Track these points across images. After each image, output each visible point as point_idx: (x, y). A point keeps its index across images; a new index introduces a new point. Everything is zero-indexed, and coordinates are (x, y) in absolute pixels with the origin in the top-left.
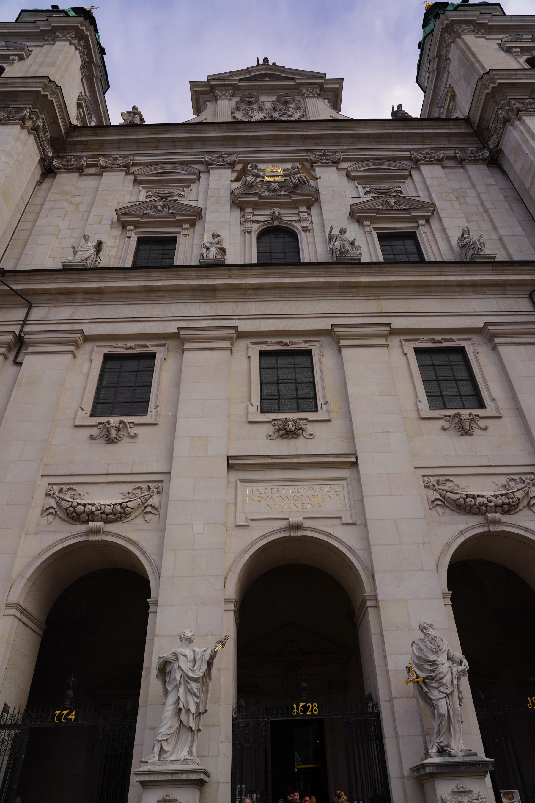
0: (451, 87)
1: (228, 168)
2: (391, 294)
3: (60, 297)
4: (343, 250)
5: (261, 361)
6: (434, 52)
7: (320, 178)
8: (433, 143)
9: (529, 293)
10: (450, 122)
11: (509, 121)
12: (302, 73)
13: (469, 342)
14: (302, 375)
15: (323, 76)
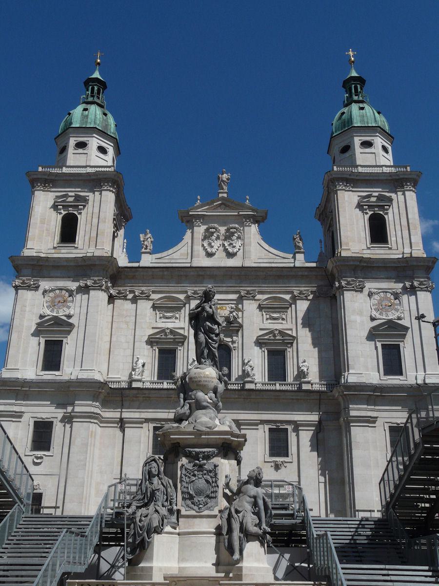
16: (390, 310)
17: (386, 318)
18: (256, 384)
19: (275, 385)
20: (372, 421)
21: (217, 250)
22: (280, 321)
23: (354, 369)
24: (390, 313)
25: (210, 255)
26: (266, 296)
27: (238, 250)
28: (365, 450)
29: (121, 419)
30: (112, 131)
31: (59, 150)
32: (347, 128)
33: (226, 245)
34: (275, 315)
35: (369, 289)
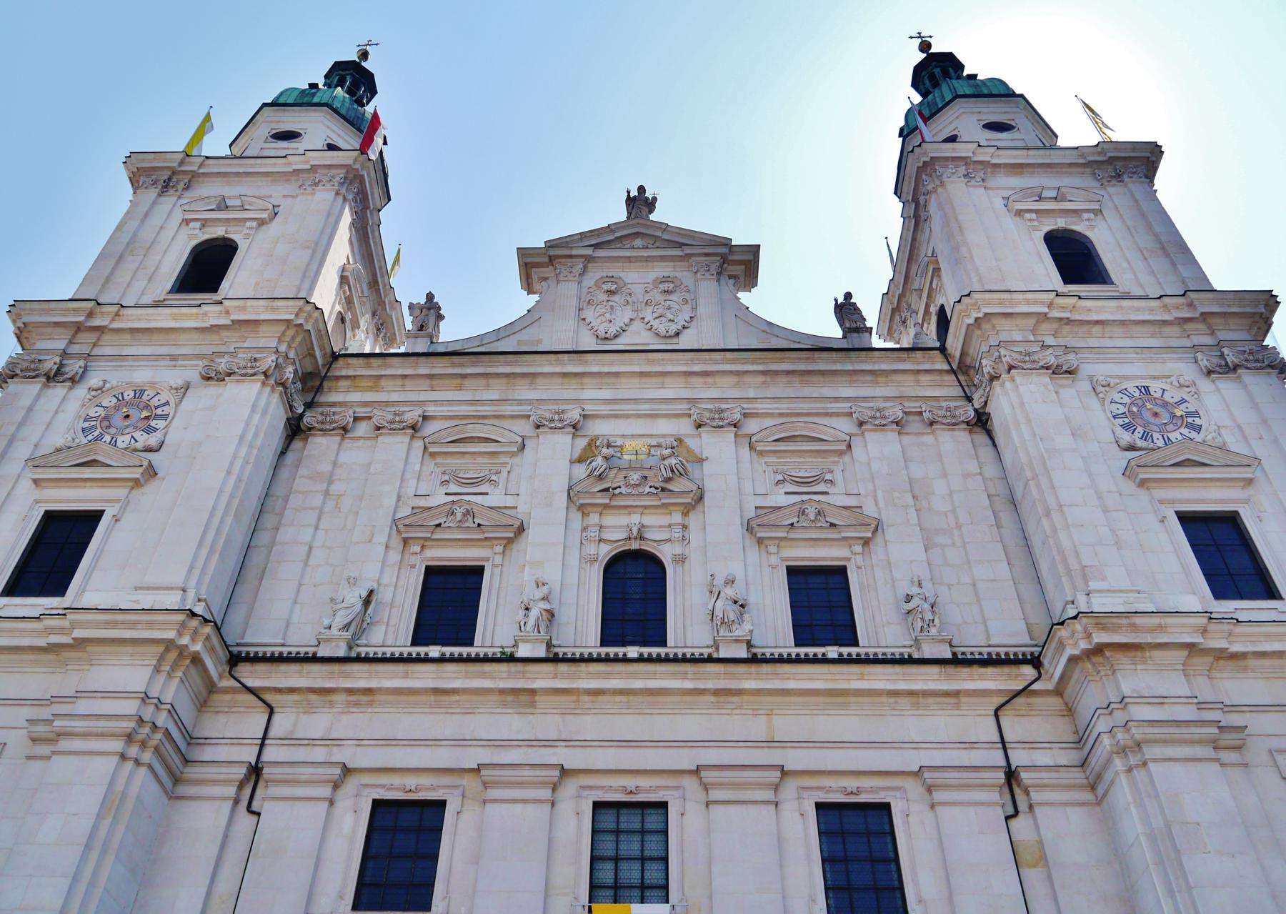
0: (935, 255)
1: (568, 433)
2: (790, 706)
3: (313, 697)
4: (726, 620)
5: (595, 818)
6: (908, 193)
7: (707, 458)
8: (890, 385)
9: (994, 708)
10: (918, 352)
11: (998, 378)
12: (694, 234)
13: (898, 794)
14: (653, 847)
15: (726, 242)
16: (1170, 427)
21: (621, 328)
23: (1104, 579)
27: (680, 328)
29: (255, 771)
33: (649, 315)
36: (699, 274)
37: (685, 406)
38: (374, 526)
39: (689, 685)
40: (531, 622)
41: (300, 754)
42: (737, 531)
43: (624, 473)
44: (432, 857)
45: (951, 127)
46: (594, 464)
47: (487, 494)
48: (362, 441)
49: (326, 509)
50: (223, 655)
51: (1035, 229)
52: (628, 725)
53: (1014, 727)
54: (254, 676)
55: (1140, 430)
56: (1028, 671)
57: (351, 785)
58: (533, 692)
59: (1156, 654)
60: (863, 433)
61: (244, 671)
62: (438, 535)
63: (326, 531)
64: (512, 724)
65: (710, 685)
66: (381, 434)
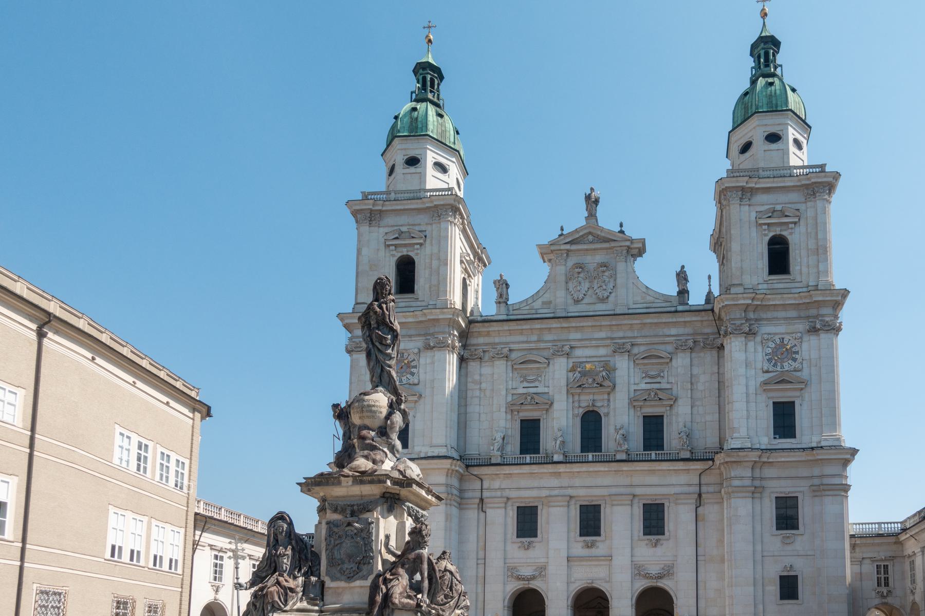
15: (630, 239)
16: (786, 360)
17: (781, 370)
18: (629, 455)
19: (651, 454)
20: (756, 491)
22: (658, 380)
24: (784, 364)
25: (577, 302)
26: (642, 348)
27: (608, 294)
28: (746, 525)
29: (482, 500)
30: (452, 140)
31: (385, 171)
32: (749, 115)
34: (652, 373)
35: (763, 334)
36: (618, 258)
37: (609, 341)
38: (500, 404)
39: (606, 469)
40: (557, 446)
41: (493, 494)
42: (627, 401)
43: (586, 378)
44: (536, 522)
45: (750, 135)
46: (575, 375)
47: (537, 387)
48: (488, 363)
49: (482, 396)
50: (463, 466)
51: (766, 235)
52: (589, 481)
53: (705, 479)
54: (476, 471)
55: (774, 362)
56: (711, 462)
57: (510, 503)
58: (560, 472)
59: (744, 463)
60: (677, 353)
61: (471, 469)
62: (523, 407)
63: (484, 406)
64: (555, 482)
65: (613, 469)
66: (495, 360)
